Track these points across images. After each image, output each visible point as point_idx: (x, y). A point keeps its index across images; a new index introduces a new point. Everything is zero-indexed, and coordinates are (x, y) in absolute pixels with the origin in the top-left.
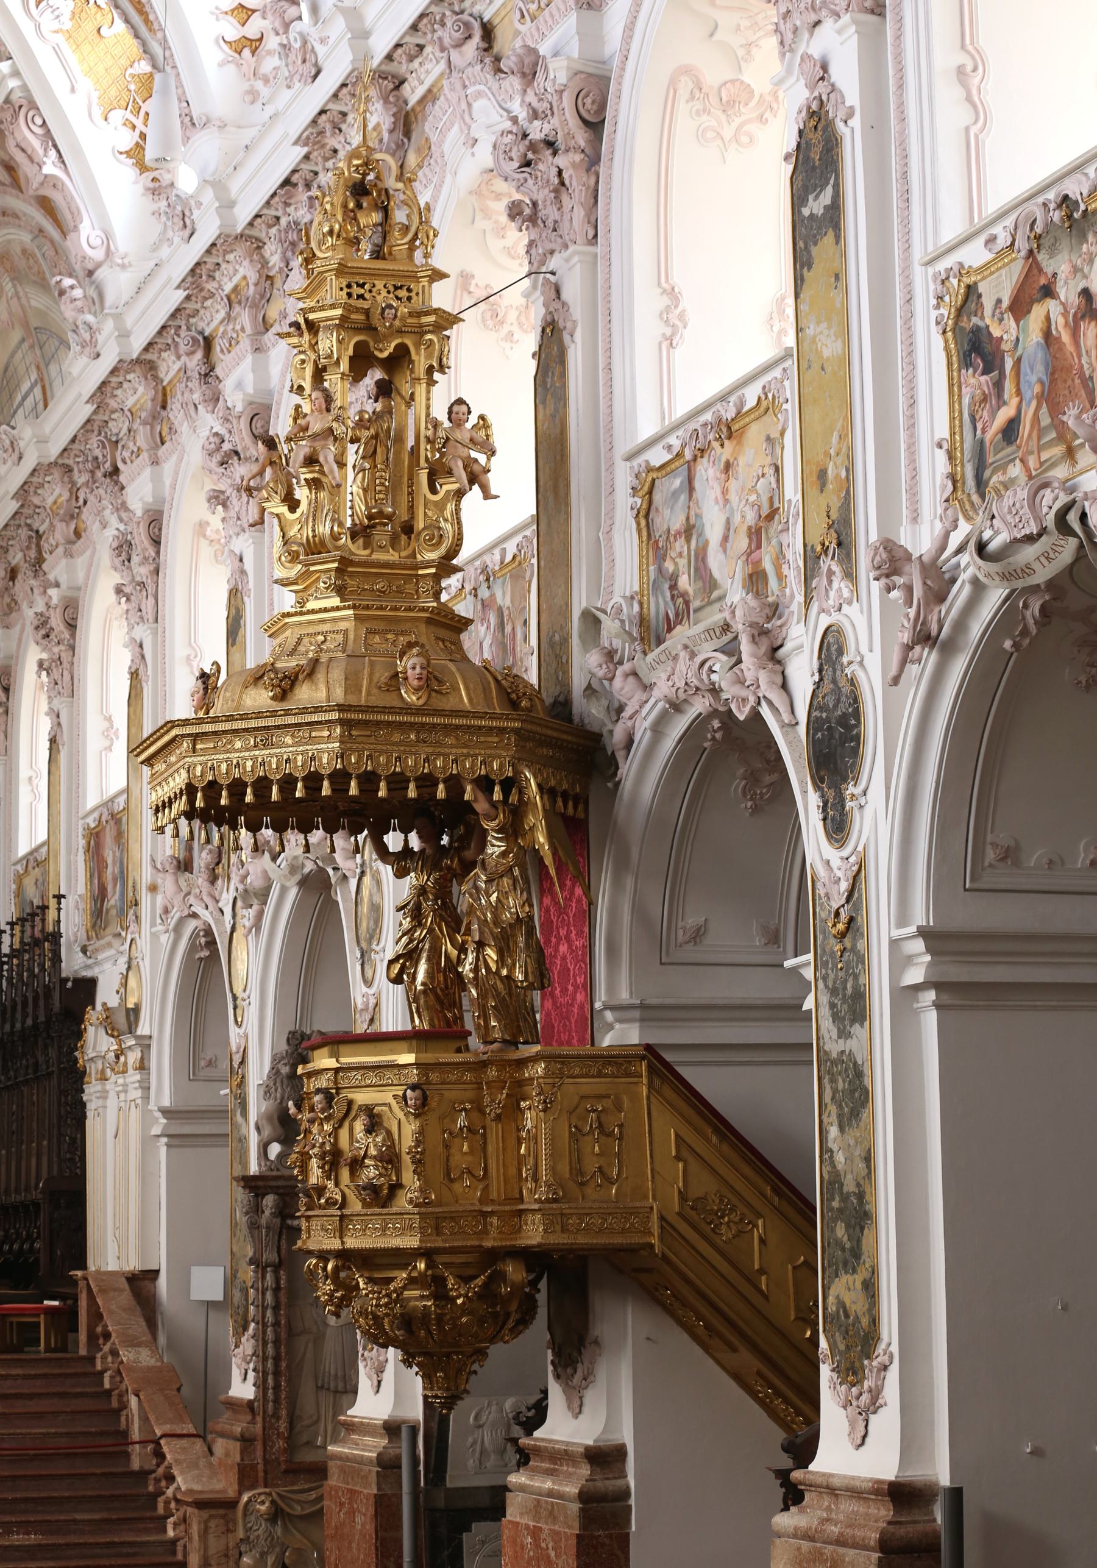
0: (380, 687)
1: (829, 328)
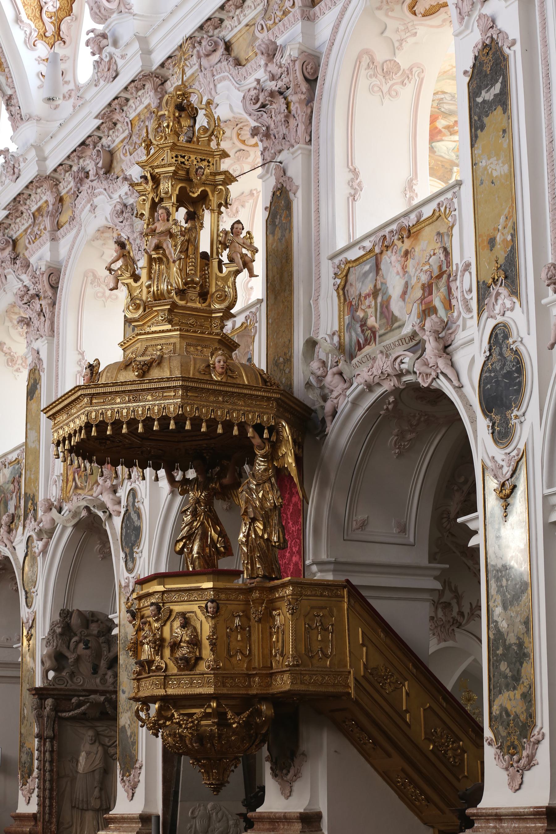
1: (497, 160)
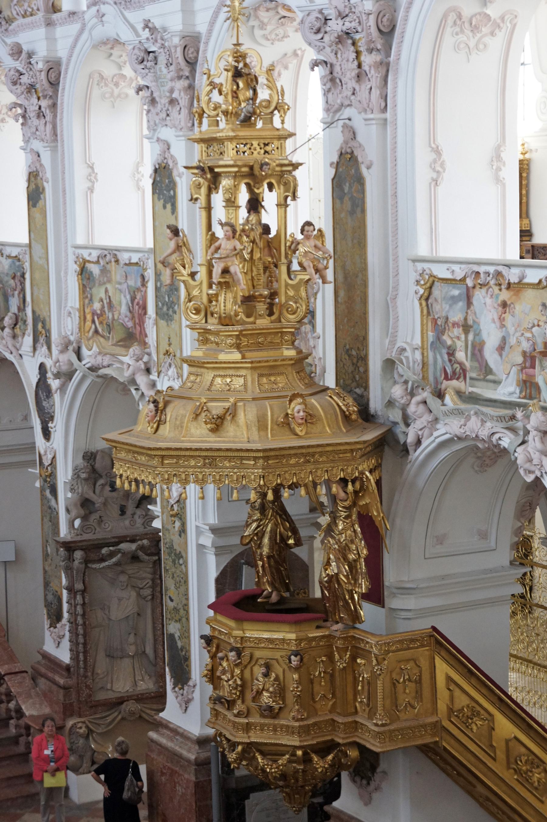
0: (278, 425)
